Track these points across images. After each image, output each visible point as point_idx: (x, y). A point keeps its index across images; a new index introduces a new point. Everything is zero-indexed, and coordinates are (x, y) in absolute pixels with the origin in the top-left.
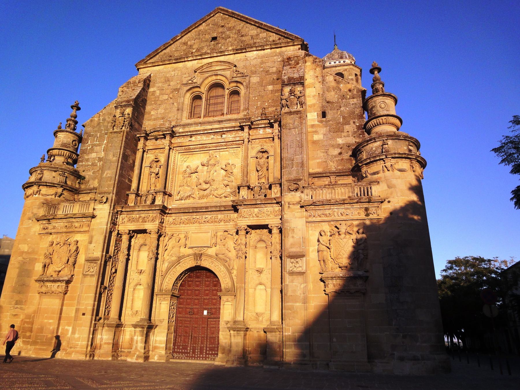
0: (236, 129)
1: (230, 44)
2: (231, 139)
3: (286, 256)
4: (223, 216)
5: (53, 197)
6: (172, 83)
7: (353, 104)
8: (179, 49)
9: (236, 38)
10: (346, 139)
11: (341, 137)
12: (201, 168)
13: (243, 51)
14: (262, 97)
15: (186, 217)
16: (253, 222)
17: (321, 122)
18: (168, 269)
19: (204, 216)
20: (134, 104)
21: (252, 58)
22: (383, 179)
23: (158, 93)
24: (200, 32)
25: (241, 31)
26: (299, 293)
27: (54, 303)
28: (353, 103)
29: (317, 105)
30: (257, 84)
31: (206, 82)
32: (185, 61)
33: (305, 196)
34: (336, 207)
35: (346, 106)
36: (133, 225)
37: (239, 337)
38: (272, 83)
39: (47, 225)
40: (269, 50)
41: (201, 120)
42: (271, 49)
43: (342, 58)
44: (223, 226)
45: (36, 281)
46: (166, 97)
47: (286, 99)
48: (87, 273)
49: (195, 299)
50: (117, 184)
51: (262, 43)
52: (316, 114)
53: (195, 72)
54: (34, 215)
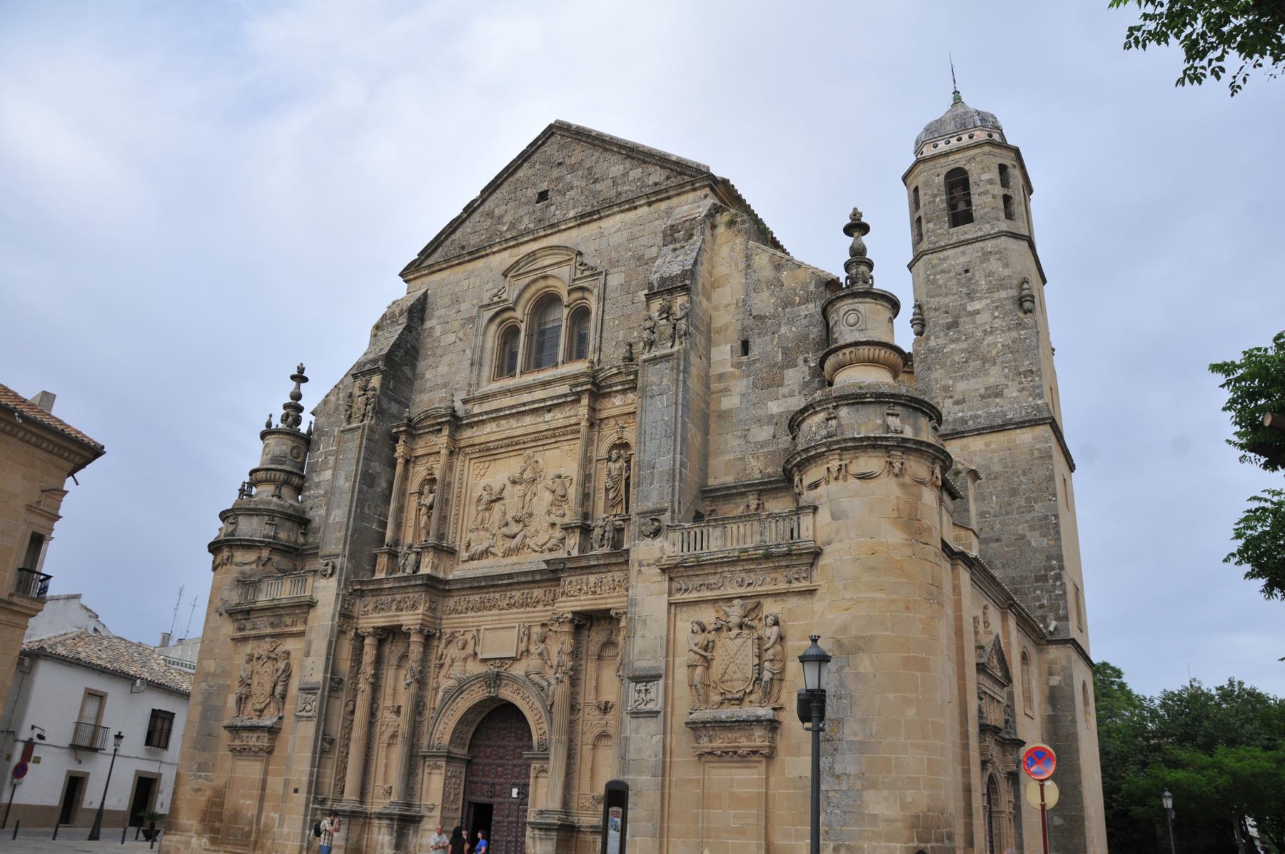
0: (569, 399)
1: (571, 202)
2: (561, 423)
3: (629, 678)
4: (542, 591)
5: (254, 566)
6: (464, 307)
7: (806, 316)
8: (478, 229)
9: (584, 188)
10: (786, 402)
11: (777, 399)
12: (510, 489)
13: (595, 217)
14: (628, 317)
15: (477, 597)
16: (585, 605)
17: (738, 365)
19: (508, 594)
20: (385, 365)
21: (613, 230)
22: (824, 499)
23: (438, 329)
24: (518, 185)
25: (595, 170)
27: (251, 770)
28: (807, 313)
29: (733, 327)
30: (619, 290)
31: (527, 295)
32: (487, 255)
33: (667, 547)
34: (726, 569)
35: (791, 322)
36: (382, 617)
37: (550, 842)
39: (244, 622)
40: (646, 209)
42: (650, 204)
43: (964, 127)
44: (540, 614)
45: (225, 727)
46: (452, 338)
47: (649, 328)
48: (301, 714)
49: (499, 766)
50: (351, 536)
51: (632, 191)
52: (729, 346)
53: (506, 276)
54: (224, 604)
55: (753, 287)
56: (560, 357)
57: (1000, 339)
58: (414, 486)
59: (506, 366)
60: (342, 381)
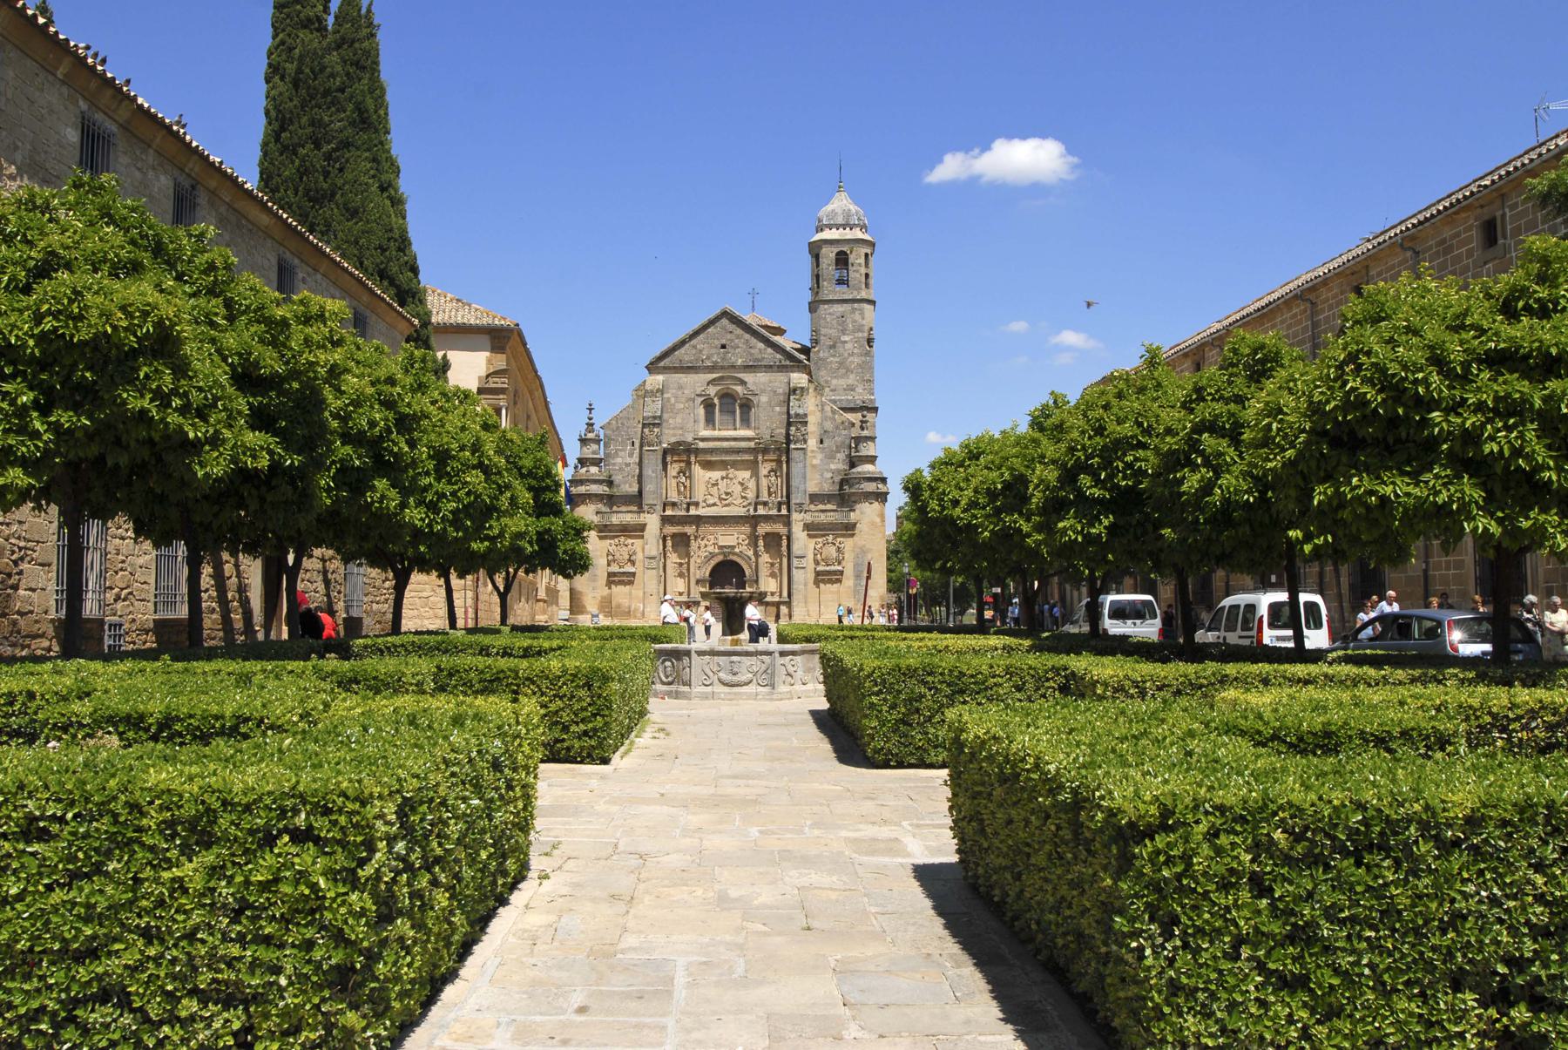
23: (673, 400)
26: (802, 580)
38: (780, 405)
41: (716, 433)
55: (824, 418)
57: (856, 360)
58: (675, 474)
59: (710, 420)
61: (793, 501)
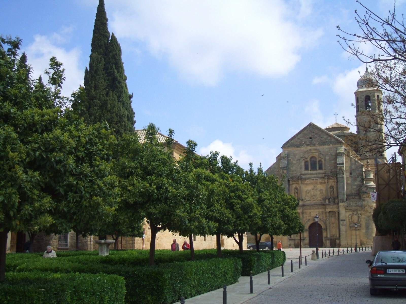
18: (306, 223)
23: (292, 160)
38: (333, 160)
46: (295, 162)
55: (351, 164)
56: (318, 168)
58: (293, 188)
59: (306, 169)
60: (271, 166)
61: (339, 198)
